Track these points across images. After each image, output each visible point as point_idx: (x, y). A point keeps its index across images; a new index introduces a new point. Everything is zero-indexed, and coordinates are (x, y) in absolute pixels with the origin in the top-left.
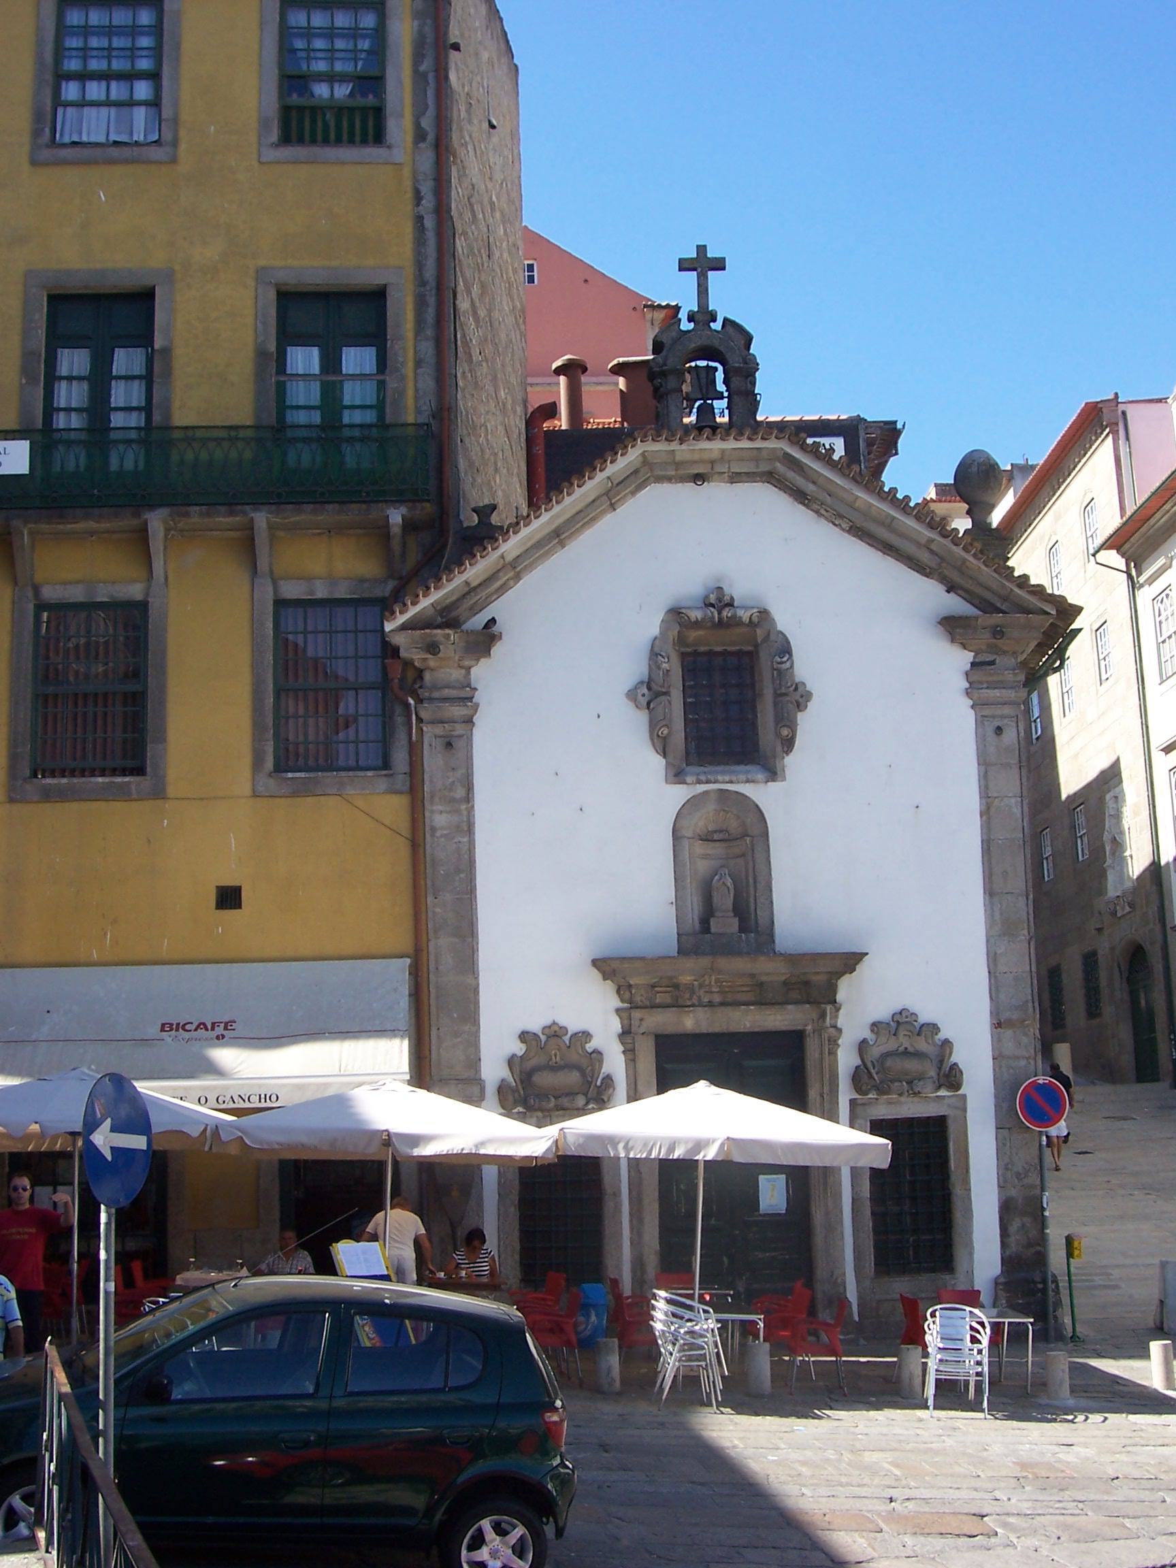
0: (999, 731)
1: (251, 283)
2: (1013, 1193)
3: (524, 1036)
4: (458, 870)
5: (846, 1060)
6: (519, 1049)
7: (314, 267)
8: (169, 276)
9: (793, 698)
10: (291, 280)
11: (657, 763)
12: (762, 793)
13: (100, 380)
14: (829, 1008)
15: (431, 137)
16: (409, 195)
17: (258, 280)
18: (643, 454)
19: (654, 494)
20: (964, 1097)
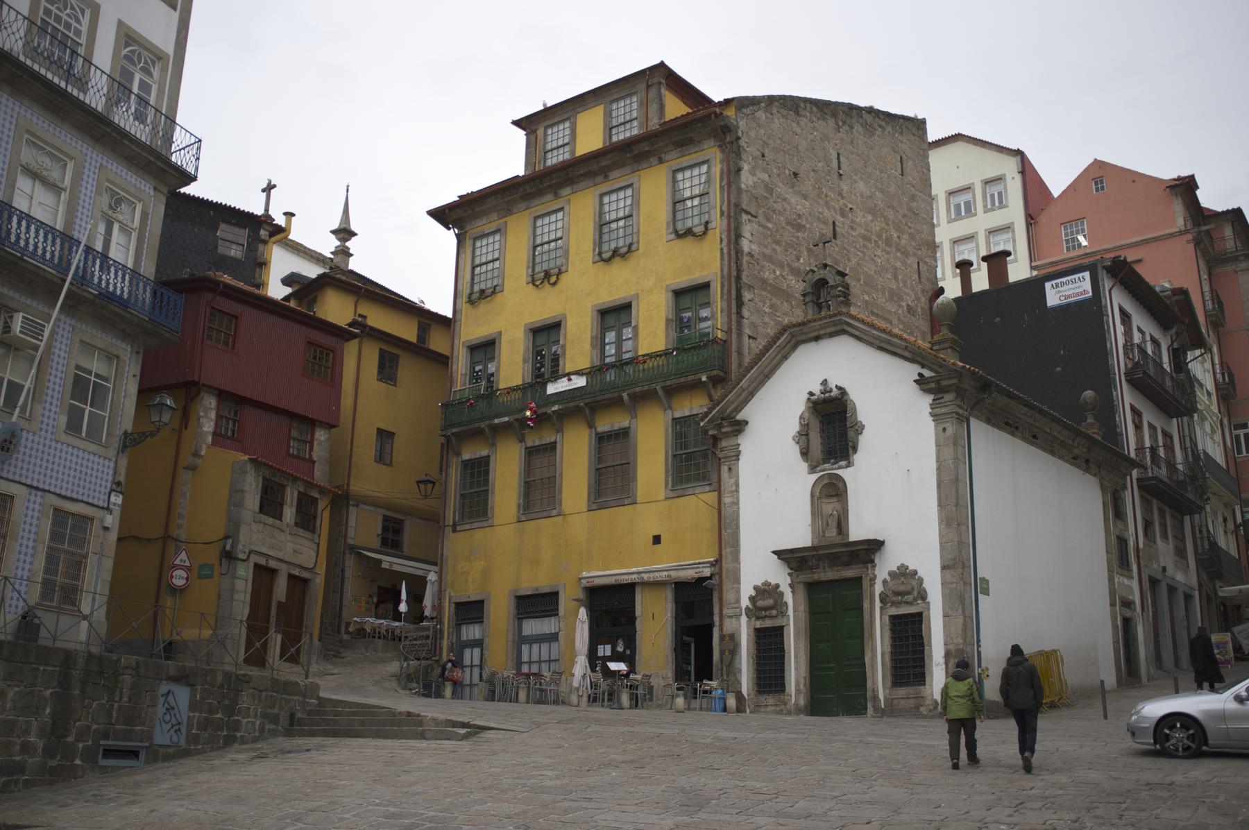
0: (944, 429)
2: (951, 647)
3: (756, 588)
5: (879, 588)
7: (683, 281)
10: (674, 287)
11: (805, 465)
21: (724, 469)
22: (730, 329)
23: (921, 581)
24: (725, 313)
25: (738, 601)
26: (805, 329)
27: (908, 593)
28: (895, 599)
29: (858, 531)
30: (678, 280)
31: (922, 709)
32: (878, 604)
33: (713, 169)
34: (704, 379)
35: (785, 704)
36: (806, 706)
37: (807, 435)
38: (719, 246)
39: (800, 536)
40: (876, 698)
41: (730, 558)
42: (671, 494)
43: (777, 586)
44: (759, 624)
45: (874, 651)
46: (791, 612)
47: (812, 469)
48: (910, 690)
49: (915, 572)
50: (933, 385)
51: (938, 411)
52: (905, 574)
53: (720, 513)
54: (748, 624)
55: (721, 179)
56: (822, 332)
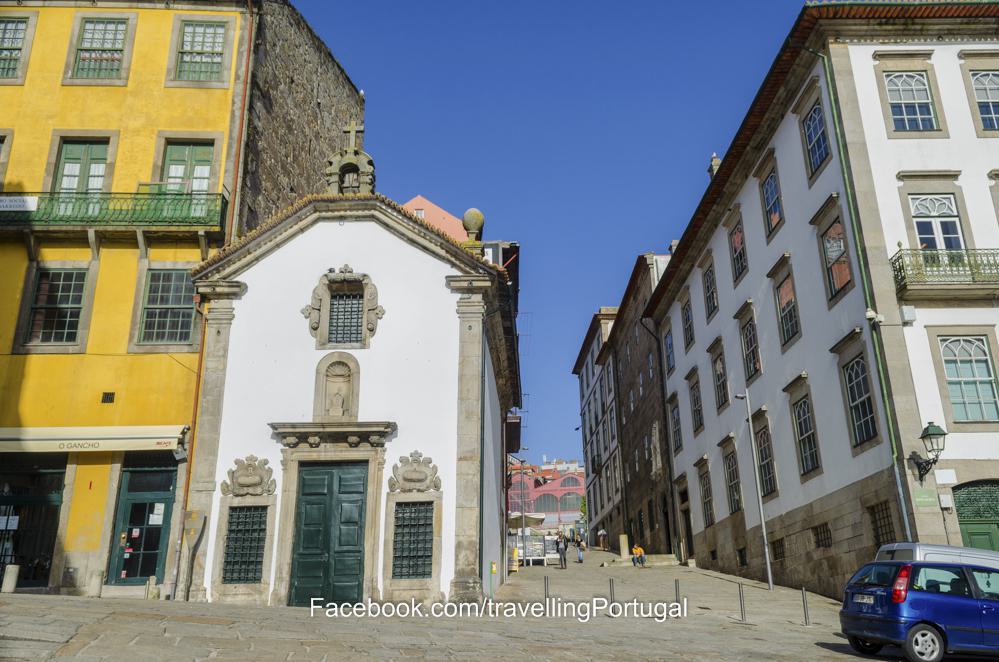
1: (154, 137)
2: (461, 538)
5: (387, 473)
6: (234, 467)
8: (118, 133)
9: (377, 312)
11: (314, 340)
12: (357, 353)
13: (85, 176)
14: (379, 449)
15: (242, 78)
16: (230, 102)
17: (159, 136)
19: (321, 225)
21: (210, 331)
23: (435, 467)
25: (212, 474)
26: (331, 205)
29: (369, 411)
30: (175, 129)
32: (385, 489)
33: (231, 33)
34: (201, 233)
37: (319, 310)
38: (230, 108)
39: (303, 412)
40: (374, 589)
42: (136, 349)
43: (266, 462)
44: (237, 502)
45: (376, 538)
46: (278, 491)
47: (321, 345)
48: (415, 582)
50: (465, 284)
51: (464, 309)
53: (199, 376)
54: (222, 501)
55: (241, 44)
56: (349, 213)
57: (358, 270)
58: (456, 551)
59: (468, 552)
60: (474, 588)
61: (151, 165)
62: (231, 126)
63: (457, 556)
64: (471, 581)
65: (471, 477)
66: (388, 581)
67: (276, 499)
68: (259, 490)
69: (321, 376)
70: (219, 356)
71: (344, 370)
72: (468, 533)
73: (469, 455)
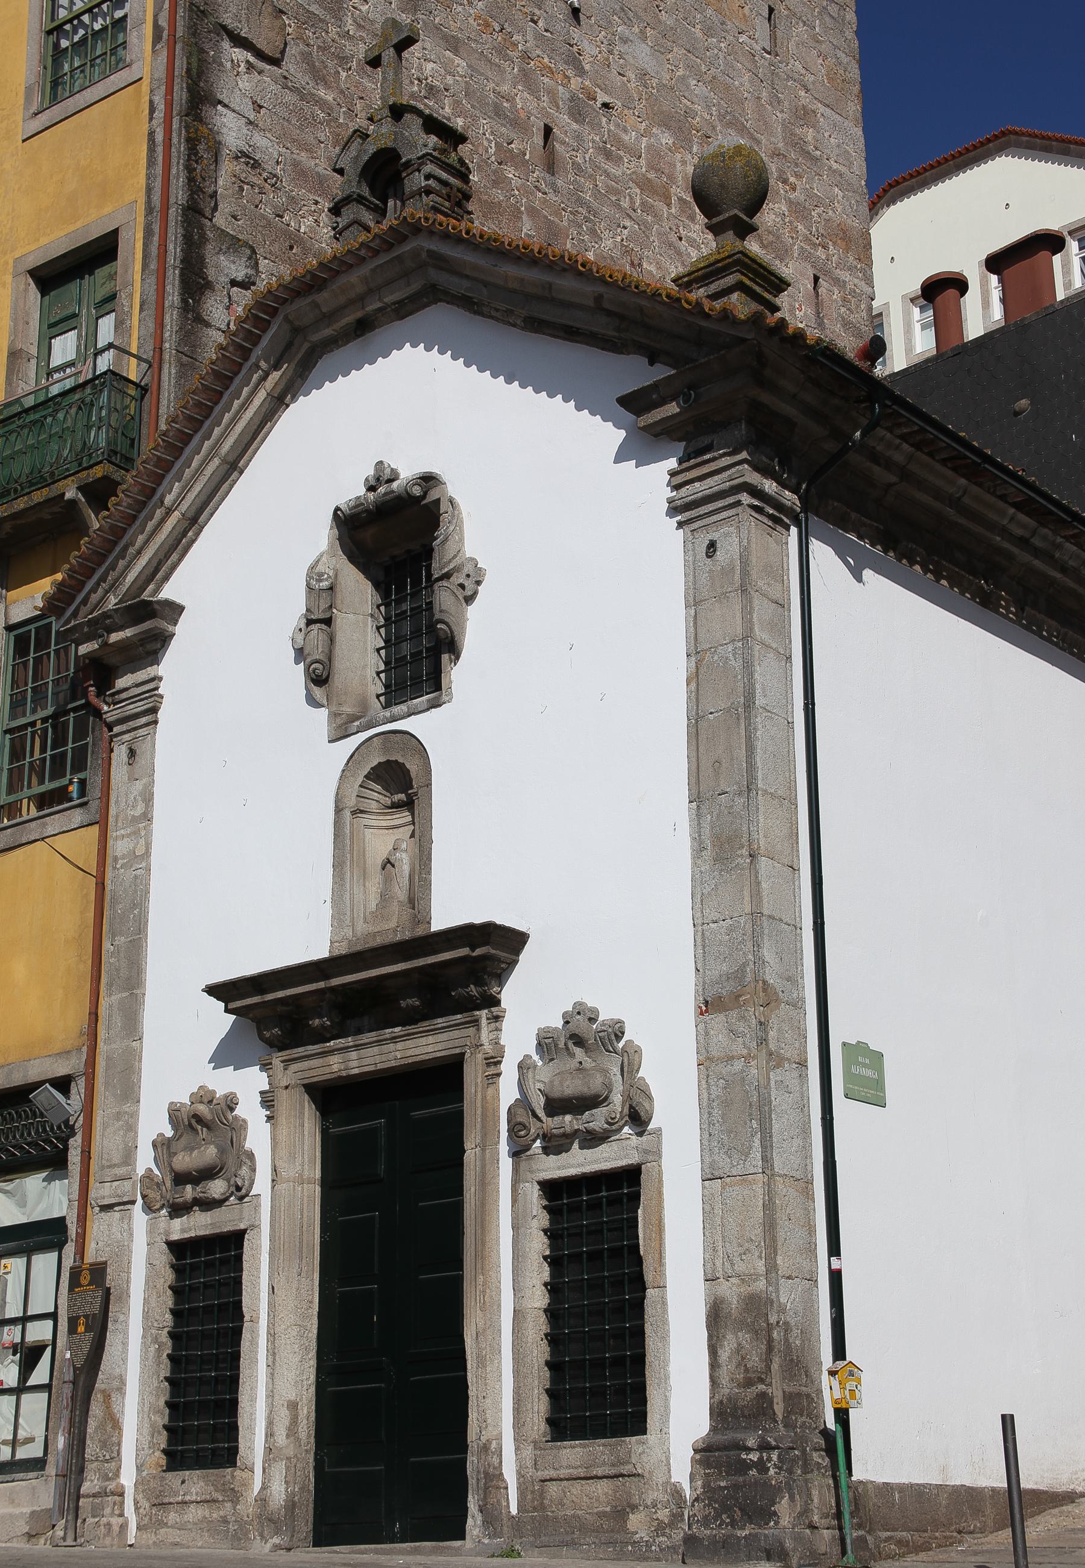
4: (134, 906)
5: (508, 1092)
7: (55, 240)
10: (34, 261)
14: (483, 1014)
18: (286, 319)
20: (658, 1132)
22: (159, 350)
24: (150, 311)
25: (129, 1156)
26: (325, 299)
27: (591, 1102)
28: (551, 1123)
30: (44, 241)
31: (636, 1522)
35: (234, 1496)
36: (291, 1505)
37: (328, 622)
38: (145, 128)
39: (298, 932)
40: (493, 1479)
41: (118, 1021)
44: (179, 1229)
46: (262, 1185)
49: (617, 1031)
52: (583, 1036)
53: (101, 886)
54: (151, 1231)
56: (373, 306)
57: (408, 471)
58: (710, 1337)
59: (745, 1337)
60: (762, 1467)
61: (6, 354)
62: (148, 177)
63: (713, 1351)
64: (751, 1443)
65: (738, 1065)
66: (528, 1451)
67: (257, 1208)
68: (217, 1188)
69: (347, 814)
70: (135, 820)
71: (397, 781)
72: (740, 1267)
73: (726, 989)
